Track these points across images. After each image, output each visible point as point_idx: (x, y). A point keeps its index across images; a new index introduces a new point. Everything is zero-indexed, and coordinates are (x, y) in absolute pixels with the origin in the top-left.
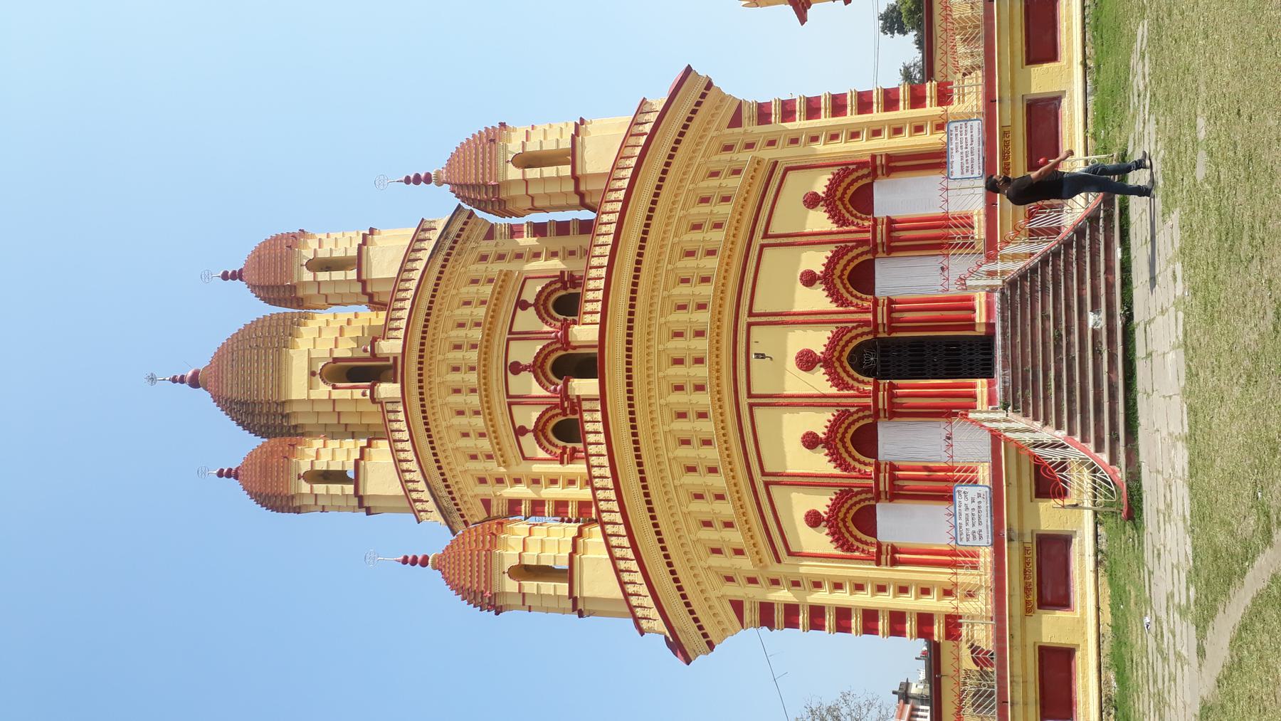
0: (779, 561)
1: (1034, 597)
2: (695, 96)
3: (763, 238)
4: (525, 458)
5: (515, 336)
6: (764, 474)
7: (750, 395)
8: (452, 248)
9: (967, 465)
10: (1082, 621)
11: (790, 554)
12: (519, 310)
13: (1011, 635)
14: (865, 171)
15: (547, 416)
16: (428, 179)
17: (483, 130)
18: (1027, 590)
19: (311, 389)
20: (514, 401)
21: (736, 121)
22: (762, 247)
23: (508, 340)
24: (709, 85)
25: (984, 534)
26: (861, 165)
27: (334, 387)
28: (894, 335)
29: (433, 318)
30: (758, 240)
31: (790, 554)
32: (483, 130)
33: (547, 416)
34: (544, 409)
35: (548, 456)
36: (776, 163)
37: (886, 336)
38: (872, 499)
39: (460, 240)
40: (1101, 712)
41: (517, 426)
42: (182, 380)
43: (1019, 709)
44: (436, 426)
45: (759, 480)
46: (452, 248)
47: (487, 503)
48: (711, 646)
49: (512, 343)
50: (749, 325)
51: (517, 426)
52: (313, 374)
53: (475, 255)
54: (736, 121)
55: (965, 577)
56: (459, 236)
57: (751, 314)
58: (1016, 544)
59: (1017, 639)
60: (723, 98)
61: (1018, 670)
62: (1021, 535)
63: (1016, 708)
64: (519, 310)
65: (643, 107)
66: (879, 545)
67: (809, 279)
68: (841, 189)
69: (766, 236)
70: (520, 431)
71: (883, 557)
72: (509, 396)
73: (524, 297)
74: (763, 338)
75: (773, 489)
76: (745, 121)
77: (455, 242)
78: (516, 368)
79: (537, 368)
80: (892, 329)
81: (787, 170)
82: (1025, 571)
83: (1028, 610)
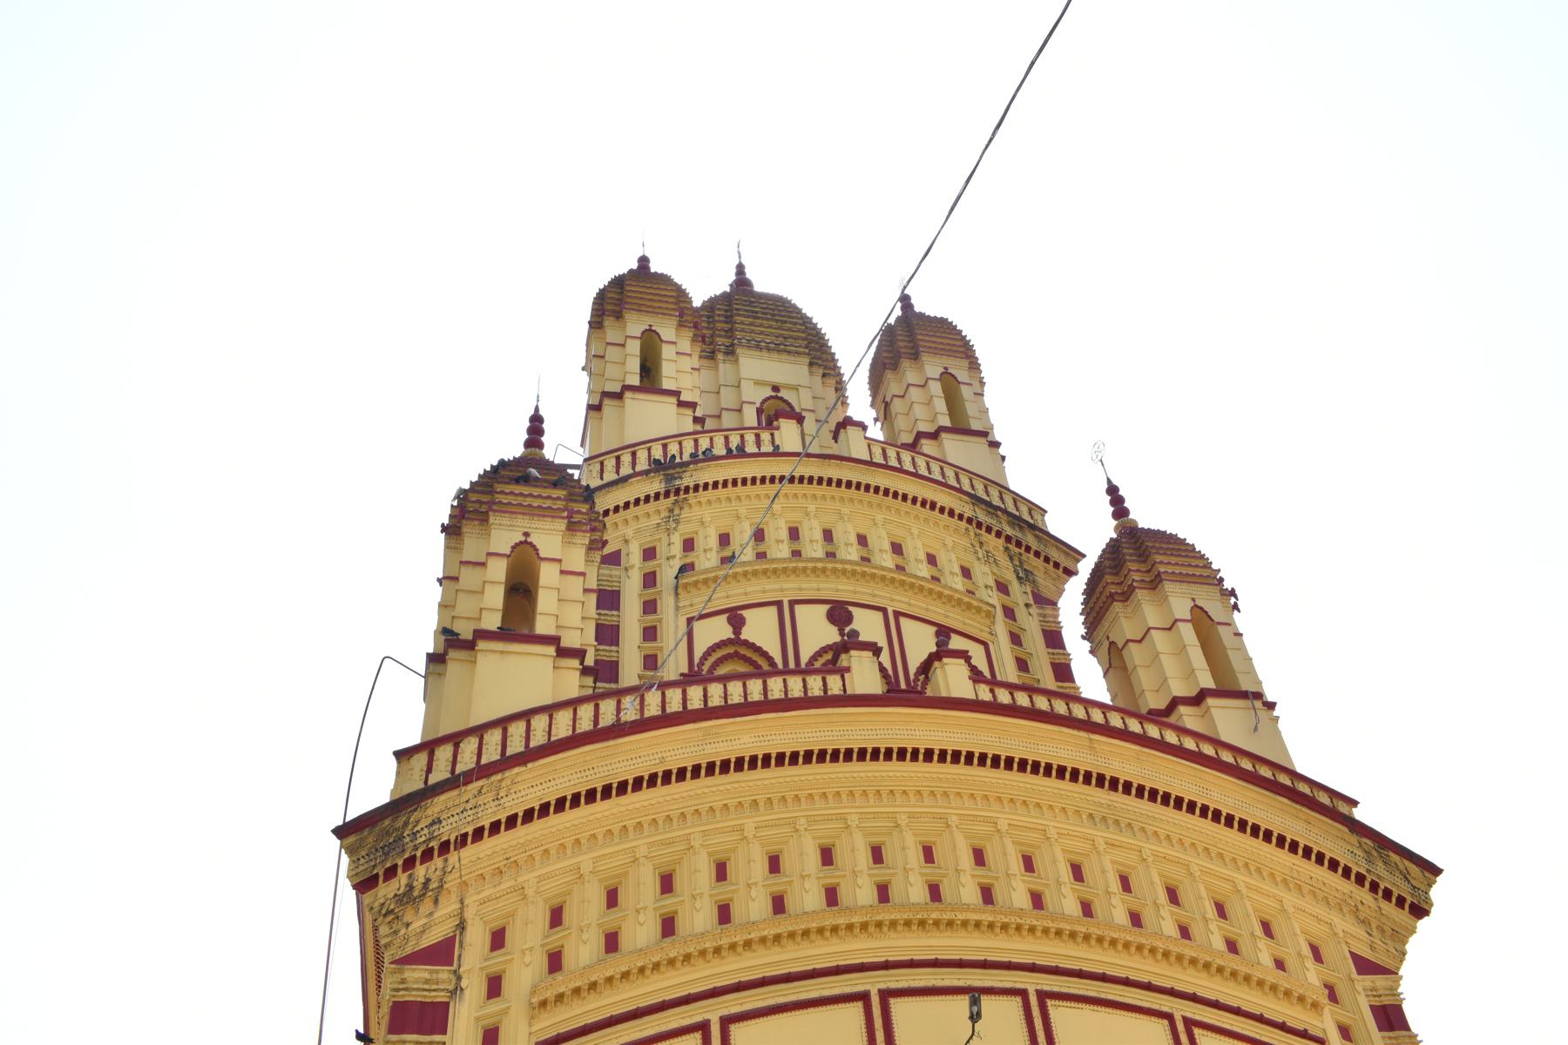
4: (690, 621)
7: (886, 995)
19: (755, 383)
20: (785, 611)
21: (1364, 966)
23: (884, 610)
24: (1420, 911)
30: (1181, 1009)
34: (771, 654)
35: (697, 660)
44: (739, 498)
50: (1023, 993)
54: (1364, 966)
60: (1400, 938)
65: (1354, 803)
70: (737, 621)
72: (793, 603)
76: (1368, 980)
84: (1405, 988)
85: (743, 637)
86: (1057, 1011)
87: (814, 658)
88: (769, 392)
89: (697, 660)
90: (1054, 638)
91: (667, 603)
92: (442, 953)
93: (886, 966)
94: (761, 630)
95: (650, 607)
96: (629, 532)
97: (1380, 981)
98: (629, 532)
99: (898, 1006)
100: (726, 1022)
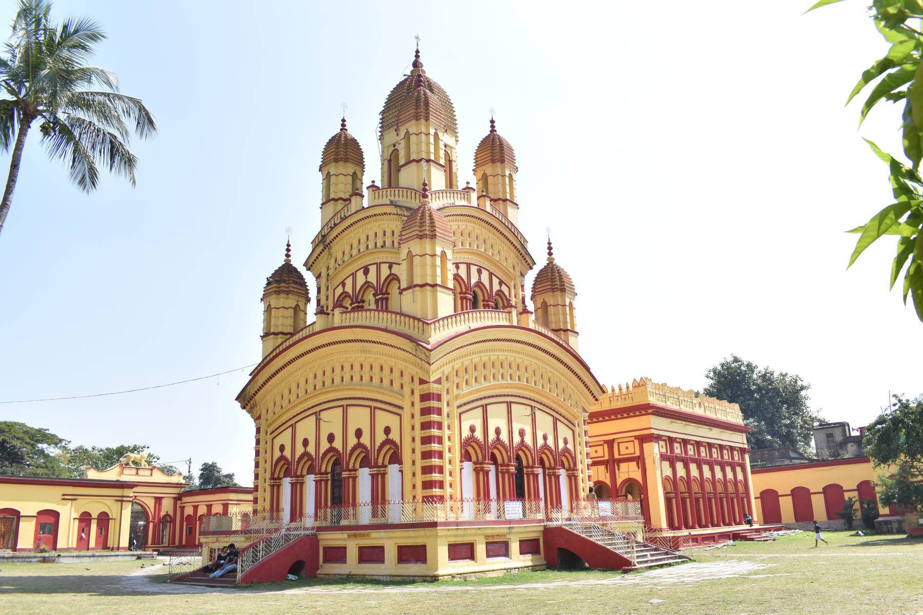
0: (459, 407)
1: (490, 540)
2: (596, 394)
5: (491, 274)
8: (521, 254)
9: (386, 511)
10: (485, 564)
11: (460, 414)
13: (480, 529)
14: (572, 466)
15: (462, 283)
16: (550, 254)
18: (493, 536)
25: (509, 516)
28: (525, 476)
29: (498, 234)
31: (460, 414)
33: (462, 283)
37: (525, 472)
39: (522, 259)
40: (460, 574)
41: (460, 265)
43: (455, 532)
46: (521, 254)
51: (460, 265)
53: (516, 265)
56: (525, 259)
58: (508, 531)
59: (479, 532)
61: (469, 532)
62: (510, 533)
63: (463, 531)
67: (472, 429)
68: (502, 449)
70: (457, 268)
77: (523, 257)
78: (479, 272)
79: (479, 284)
80: (528, 475)
81: (573, 431)
82: (498, 535)
83: (487, 537)
92: (439, 381)
93: (512, 396)
100: (486, 405)
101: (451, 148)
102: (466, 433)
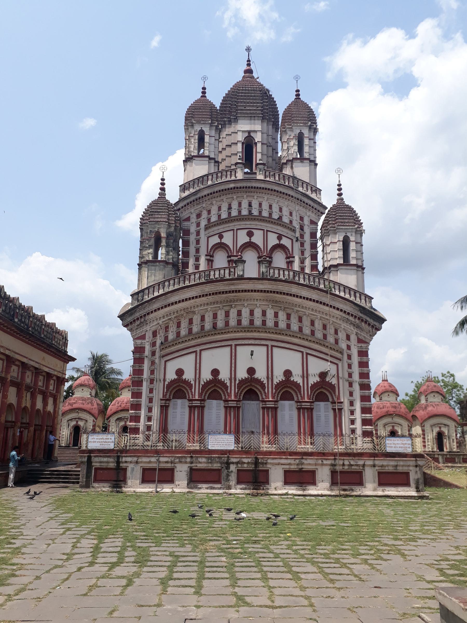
3: (306, 353)
4: (208, 238)
5: (266, 233)
6: (201, 351)
7: (236, 345)
11: (166, 362)
12: (278, 235)
17: (361, 221)
22: (302, 352)
23: (263, 230)
24: (378, 329)
26: (339, 398)
27: (243, 143)
31: (166, 362)
32: (361, 221)
35: (209, 249)
36: (340, 360)
38: (189, 397)
41: (222, 234)
42: (249, 65)
45: (198, 349)
47: (188, 219)
48: (126, 326)
49: (262, 232)
51: (222, 234)
52: (249, 132)
53: (303, 215)
55: (154, 437)
57: (272, 346)
64: (278, 235)
66: (169, 400)
69: (307, 354)
70: (221, 237)
71: (164, 402)
72: (237, 229)
73: (283, 238)
74: (261, 352)
75: (193, 355)
76: (360, 345)
78: (250, 234)
81: (337, 365)
84: (370, 347)
85: (222, 241)
86: (275, 350)
87: (241, 246)
88: (246, 134)
89: (209, 251)
90: (313, 235)
91: (202, 233)
94: (228, 239)
95: (198, 233)
96: (192, 211)
97: (363, 345)
98: (192, 211)
99: (238, 348)
101: (255, 132)
102: (171, 376)
